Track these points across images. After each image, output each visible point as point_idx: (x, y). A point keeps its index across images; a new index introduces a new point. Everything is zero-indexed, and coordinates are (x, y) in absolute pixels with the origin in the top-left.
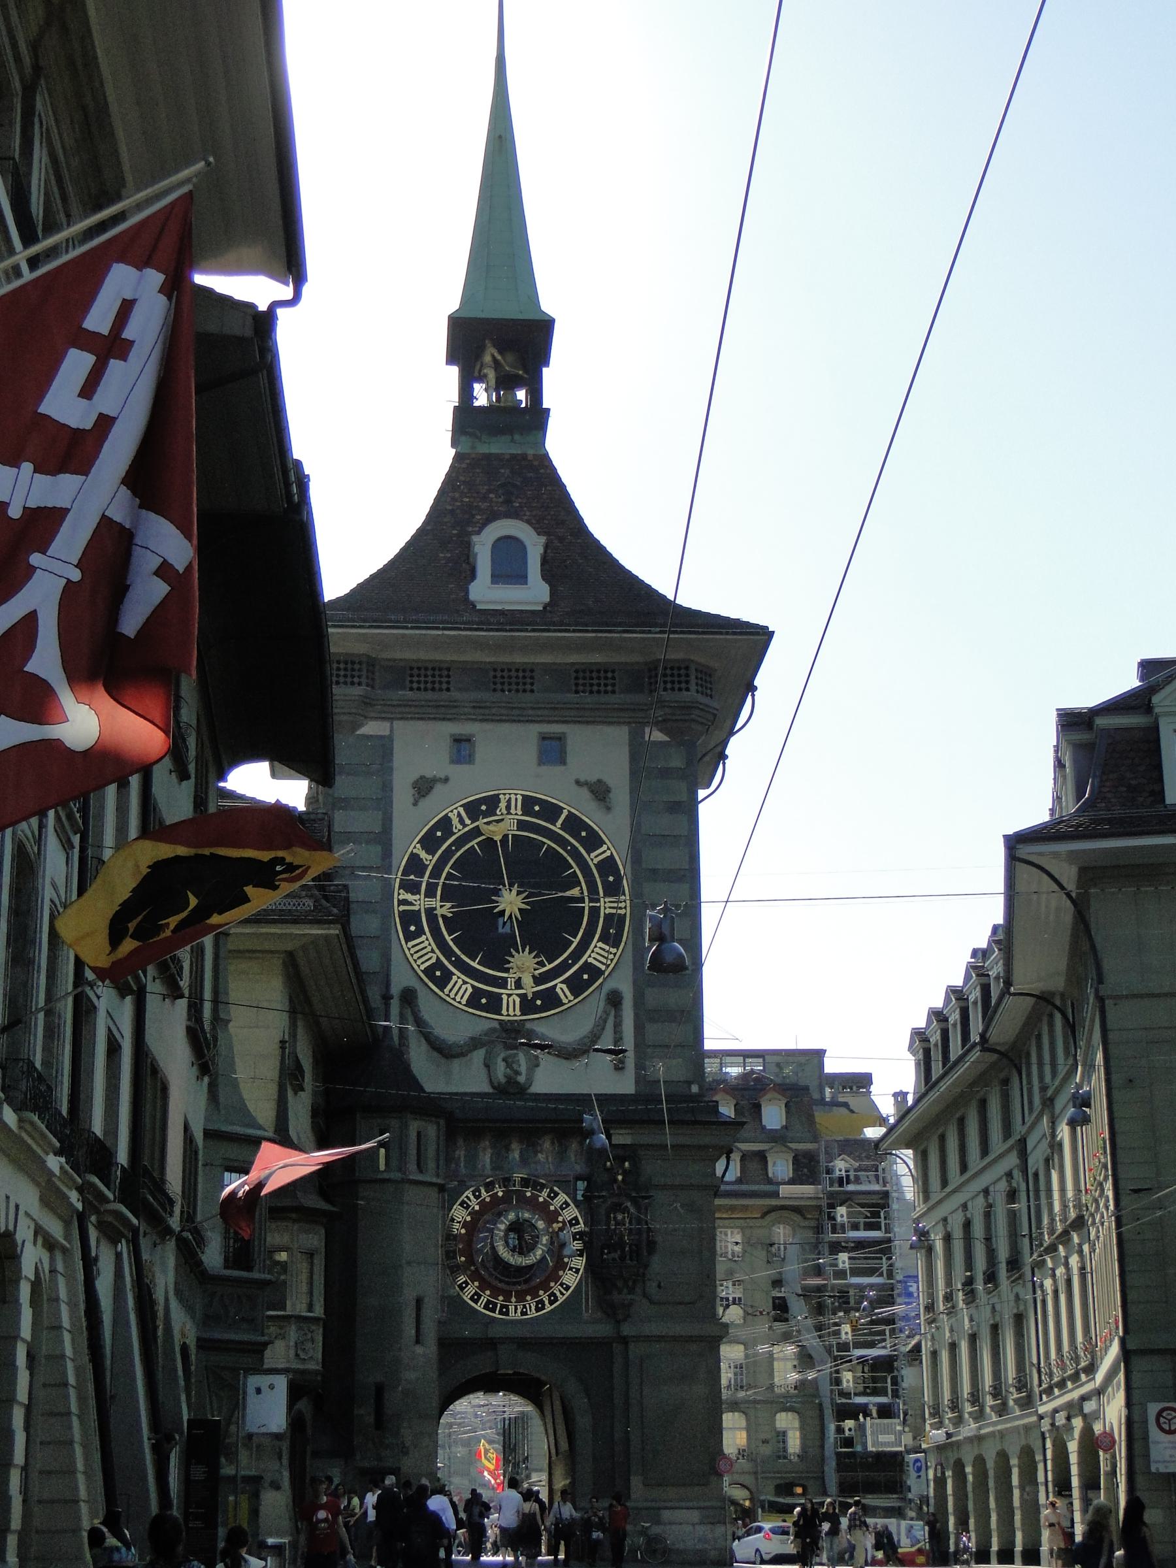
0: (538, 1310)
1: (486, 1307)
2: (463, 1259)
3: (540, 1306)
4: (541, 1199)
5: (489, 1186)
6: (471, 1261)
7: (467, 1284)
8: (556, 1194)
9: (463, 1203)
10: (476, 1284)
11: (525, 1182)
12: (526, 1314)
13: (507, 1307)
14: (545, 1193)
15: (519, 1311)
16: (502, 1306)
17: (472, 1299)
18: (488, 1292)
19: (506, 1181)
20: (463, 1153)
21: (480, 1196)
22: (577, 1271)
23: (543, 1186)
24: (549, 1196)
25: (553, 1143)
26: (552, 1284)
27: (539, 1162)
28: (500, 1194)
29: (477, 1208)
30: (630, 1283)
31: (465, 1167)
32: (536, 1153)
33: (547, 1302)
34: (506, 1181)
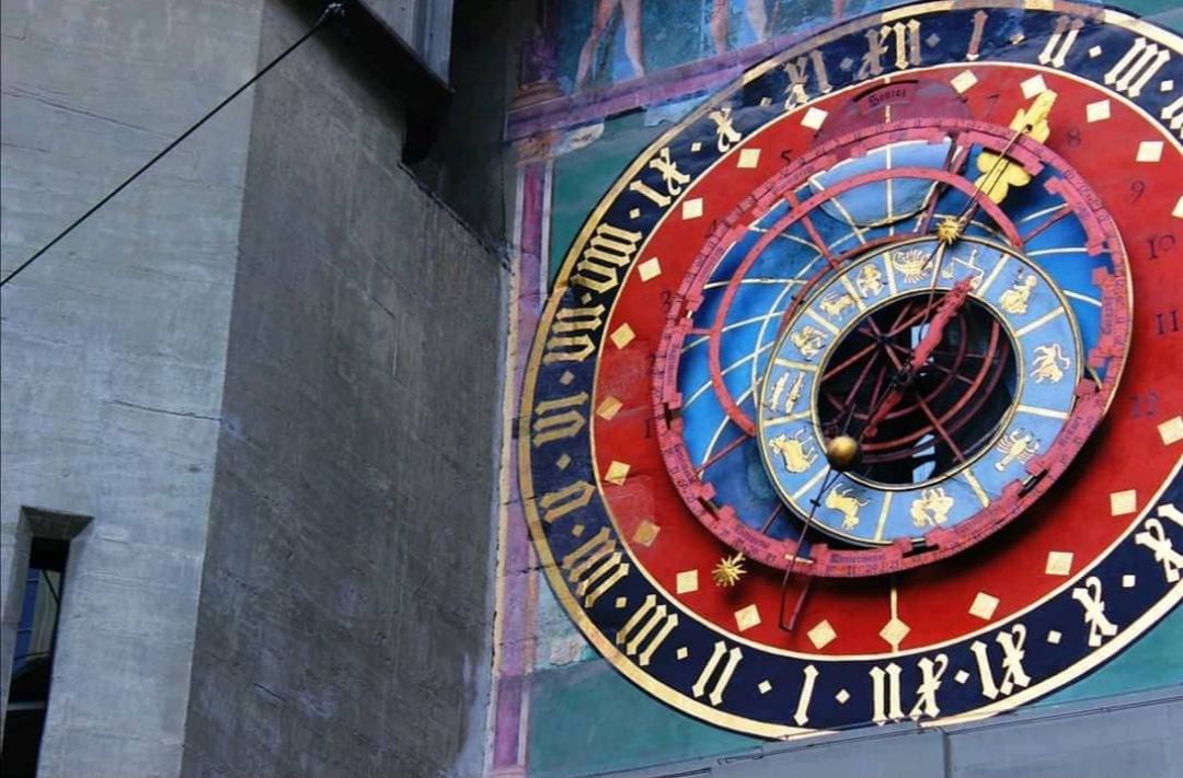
0: (1040, 663)
1: (739, 699)
2: (619, 470)
3: (1055, 639)
6: (652, 472)
7: (634, 588)
8: (1118, 44)
12: (972, 697)
13: (858, 678)
14: (1055, 52)
15: (930, 686)
16: (831, 677)
17: (662, 667)
21: (710, 152)
24: (1077, 63)
26: (1123, 502)
28: (815, 119)
29: (694, 209)
31: (643, 44)
33: (1095, 611)
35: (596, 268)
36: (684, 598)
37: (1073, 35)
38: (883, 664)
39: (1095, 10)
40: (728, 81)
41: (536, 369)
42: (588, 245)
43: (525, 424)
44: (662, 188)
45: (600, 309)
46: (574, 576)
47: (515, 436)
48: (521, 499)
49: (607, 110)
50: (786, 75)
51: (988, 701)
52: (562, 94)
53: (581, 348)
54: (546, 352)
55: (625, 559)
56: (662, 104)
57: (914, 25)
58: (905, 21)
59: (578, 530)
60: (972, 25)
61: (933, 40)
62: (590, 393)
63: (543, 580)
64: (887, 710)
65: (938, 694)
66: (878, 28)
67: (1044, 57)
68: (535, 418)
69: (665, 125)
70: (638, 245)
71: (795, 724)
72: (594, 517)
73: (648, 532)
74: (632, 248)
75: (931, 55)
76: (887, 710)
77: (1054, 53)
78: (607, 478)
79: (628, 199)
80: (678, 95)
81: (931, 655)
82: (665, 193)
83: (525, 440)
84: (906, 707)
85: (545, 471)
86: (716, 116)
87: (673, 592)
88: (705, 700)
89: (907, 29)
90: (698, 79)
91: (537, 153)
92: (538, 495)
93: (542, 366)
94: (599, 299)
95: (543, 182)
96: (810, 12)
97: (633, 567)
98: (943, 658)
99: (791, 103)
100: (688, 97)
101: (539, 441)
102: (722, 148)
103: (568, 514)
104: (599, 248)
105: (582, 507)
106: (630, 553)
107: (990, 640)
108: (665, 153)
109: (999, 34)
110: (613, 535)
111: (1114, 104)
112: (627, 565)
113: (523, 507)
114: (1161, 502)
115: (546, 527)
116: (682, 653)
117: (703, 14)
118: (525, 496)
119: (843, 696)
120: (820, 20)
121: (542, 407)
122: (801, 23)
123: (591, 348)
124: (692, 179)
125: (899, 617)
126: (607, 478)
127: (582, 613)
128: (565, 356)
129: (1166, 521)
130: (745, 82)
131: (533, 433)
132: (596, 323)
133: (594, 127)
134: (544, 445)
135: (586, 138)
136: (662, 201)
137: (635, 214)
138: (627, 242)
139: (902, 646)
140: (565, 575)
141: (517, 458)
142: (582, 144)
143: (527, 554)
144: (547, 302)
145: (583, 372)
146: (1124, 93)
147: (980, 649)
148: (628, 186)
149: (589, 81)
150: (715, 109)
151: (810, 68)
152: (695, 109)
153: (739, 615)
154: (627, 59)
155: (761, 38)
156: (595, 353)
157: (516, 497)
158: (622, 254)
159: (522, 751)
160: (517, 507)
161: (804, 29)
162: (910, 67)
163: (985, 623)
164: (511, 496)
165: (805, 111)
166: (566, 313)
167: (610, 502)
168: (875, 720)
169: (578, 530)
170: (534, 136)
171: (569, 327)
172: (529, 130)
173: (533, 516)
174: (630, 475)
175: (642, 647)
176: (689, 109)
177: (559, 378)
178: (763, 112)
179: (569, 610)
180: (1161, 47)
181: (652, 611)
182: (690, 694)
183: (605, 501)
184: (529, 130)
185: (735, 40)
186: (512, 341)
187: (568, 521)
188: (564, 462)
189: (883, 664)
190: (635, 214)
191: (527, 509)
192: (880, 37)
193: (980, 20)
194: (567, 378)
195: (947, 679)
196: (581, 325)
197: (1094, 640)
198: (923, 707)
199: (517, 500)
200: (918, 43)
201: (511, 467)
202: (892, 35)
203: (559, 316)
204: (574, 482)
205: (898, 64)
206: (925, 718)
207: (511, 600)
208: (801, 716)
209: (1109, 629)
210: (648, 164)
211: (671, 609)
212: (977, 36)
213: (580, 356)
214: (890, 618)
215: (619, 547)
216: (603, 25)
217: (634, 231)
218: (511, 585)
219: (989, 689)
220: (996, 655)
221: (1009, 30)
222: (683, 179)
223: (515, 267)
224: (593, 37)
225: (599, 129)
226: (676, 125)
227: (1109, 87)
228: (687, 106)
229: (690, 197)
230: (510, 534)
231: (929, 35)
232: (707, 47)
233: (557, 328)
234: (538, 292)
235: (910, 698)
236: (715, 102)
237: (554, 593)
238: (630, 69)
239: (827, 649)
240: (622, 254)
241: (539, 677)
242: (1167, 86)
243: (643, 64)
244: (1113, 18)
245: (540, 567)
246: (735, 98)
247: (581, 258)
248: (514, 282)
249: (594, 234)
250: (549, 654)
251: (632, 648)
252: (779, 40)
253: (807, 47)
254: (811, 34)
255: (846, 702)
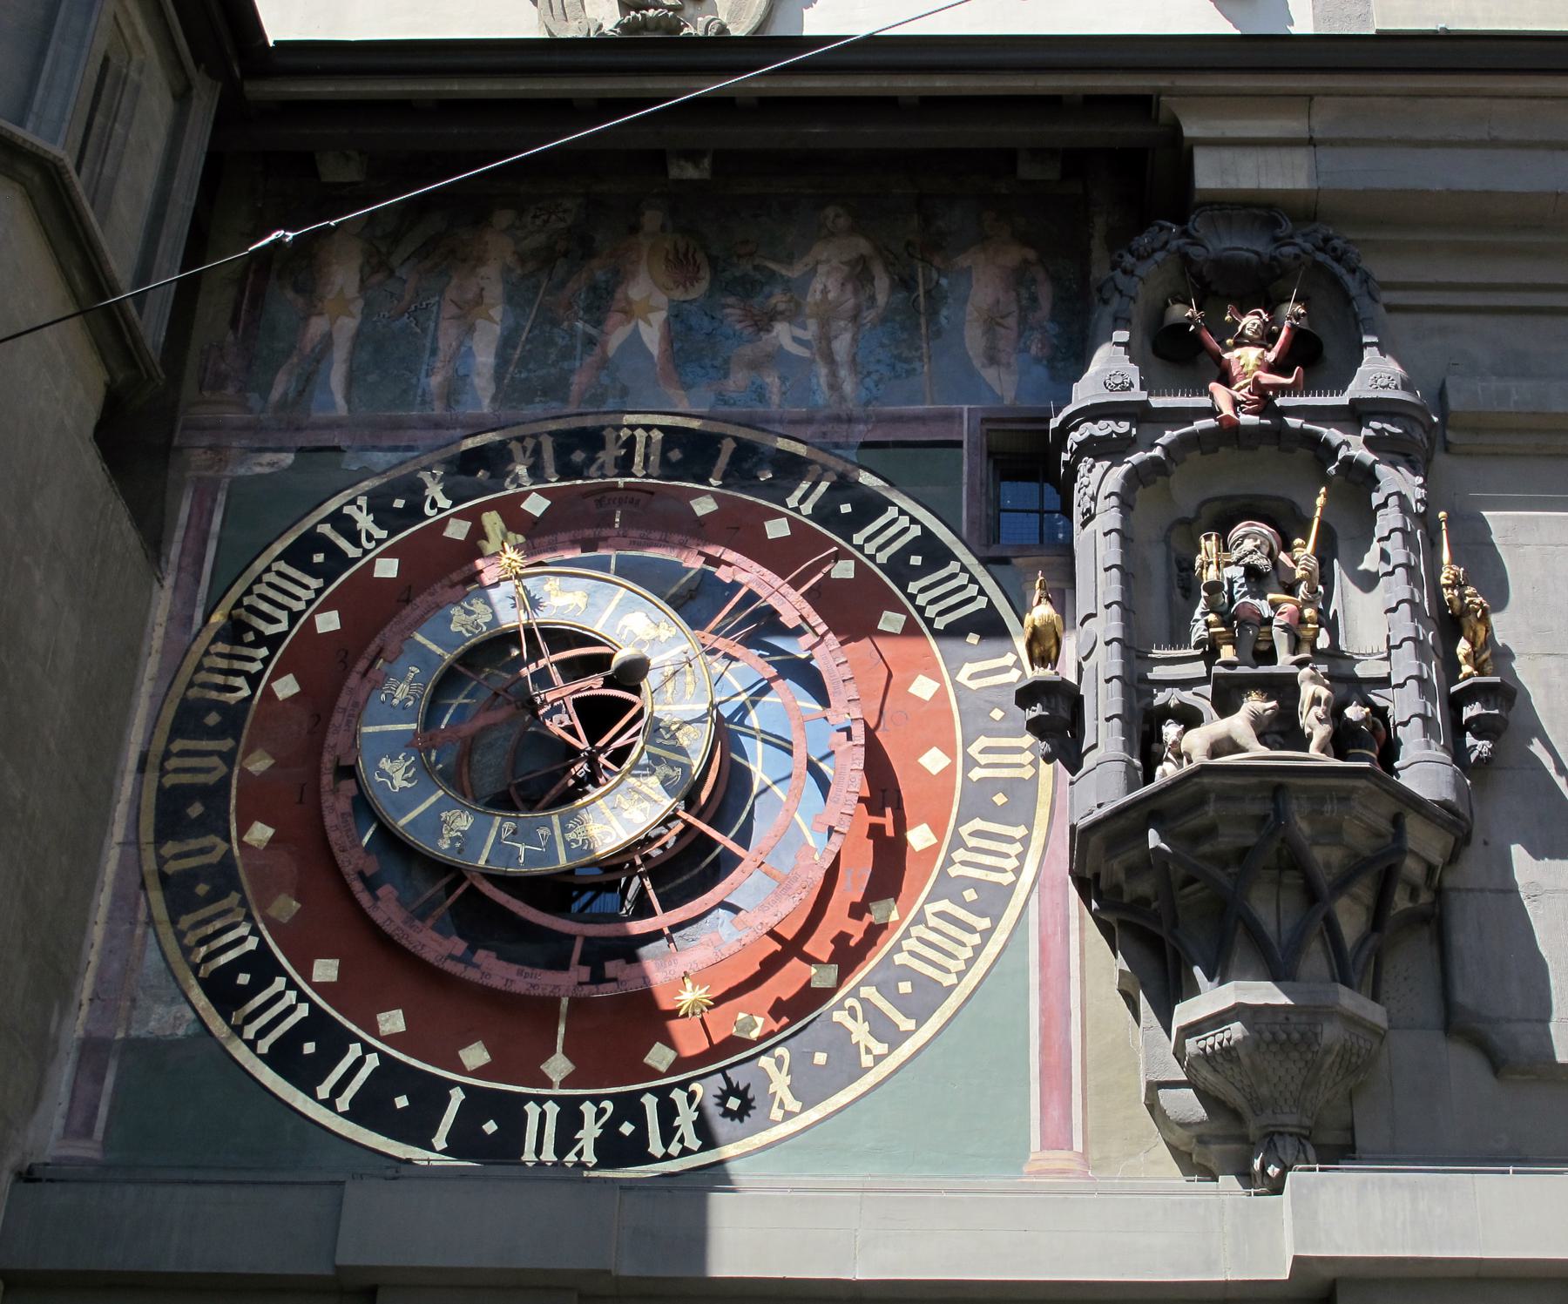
2: (260, 833)
4: (777, 529)
5: (475, 469)
7: (262, 966)
8: (870, 507)
9: (312, 541)
10: (326, 970)
11: (691, 452)
12: (636, 1151)
13: (511, 1112)
14: (803, 500)
15: (590, 1133)
17: (283, 1058)
18: (393, 1021)
19: (578, 446)
20: (348, 325)
21: (414, 512)
22: (993, 899)
23: (791, 469)
24: (825, 513)
25: (860, 275)
27: (778, 357)
29: (388, 569)
30: (1351, 919)
31: (351, 380)
32: (764, 321)
34: (578, 446)
35: (265, 607)
36: (320, 988)
37: (823, 486)
38: (540, 1100)
39: (849, 467)
40: (441, 442)
41: (177, 701)
42: (258, 580)
43: (154, 760)
44: (354, 539)
45: (263, 652)
46: (190, 939)
47: (142, 767)
48: (137, 843)
49: (302, 440)
50: (510, 452)
51: (652, 1159)
52: (250, 411)
53: (237, 689)
54: (191, 685)
55: (255, 931)
56: (364, 449)
57: (657, 435)
58: (648, 428)
59: (202, 889)
60: (719, 451)
61: (676, 455)
62: (238, 741)
63: (152, 939)
64: (539, 1150)
65: (598, 1142)
66: (619, 428)
67: (792, 501)
68: (167, 755)
69: (366, 473)
70: (319, 592)
71: (432, 1149)
72: (224, 878)
73: (287, 907)
74: (311, 595)
75: (670, 470)
76: (539, 1150)
77: (803, 500)
78: (246, 838)
79: (312, 541)
80: (386, 443)
81: (596, 1100)
82: (356, 542)
83: (152, 777)
84: (562, 1148)
85: (174, 813)
86: (425, 476)
87: (307, 977)
88: (329, 1104)
89: (649, 438)
90: (410, 432)
91: (210, 467)
92: (161, 837)
93: (184, 700)
94: (261, 640)
95: (214, 500)
96: (545, 394)
97: (262, 942)
98: (608, 1105)
99: (512, 482)
100: (395, 449)
101: (170, 780)
102: (427, 510)
103: (192, 869)
104: (271, 585)
105: (210, 865)
106: (262, 926)
107: (663, 1093)
108: (362, 501)
109: (746, 466)
110: (243, 902)
111: (859, 565)
112: (257, 939)
113: (139, 849)
114: (862, 983)
115: (164, 879)
116: (309, 1048)
117: (425, 367)
118: (143, 839)
119: (490, 1127)
120: (554, 404)
121: (178, 745)
122: (532, 402)
123: (246, 692)
124: (390, 536)
125: (565, 1052)
126: (246, 838)
127: (193, 981)
128: (214, 695)
129: (865, 1002)
130: (463, 448)
131: (163, 772)
132: (257, 666)
133: (282, 456)
134: (175, 787)
135: (271, 464)
136: (353, 552)
137: (319, 558)
138: (306, 587)
139: (563, 1085)
140: (180, 935)
141: (140, 796)
142: (267, 470)
143: (137, 904)
144: (200, 631)
145: (233, 718)
146: (872, 558)
147: (650, 1102)
148: (315, 526)
149: (283, 404)
150: (428, 468)
151: (537, 451)
152: (402, 463)
153: (381, 1017)
154: (331, 393)
155: (486, 407)
156: (250, 699)
157: (132, 837)
158: (298, 599)
159: (100, 1124)
160: (132, 850)
161: (537, 409)
162: (647, 476)
163: (658, 1075)
164: (126, 836)
165: (527, 494)
166: (221, 647)
167: (246, 866)
168: (524, 1158)
169: (202, 889)
170: (210, 448)
171: (223, 664)
172: (206, 441)
173: (150, 864)
174: (272, 840)
175: (262, 1033)
176: (395, 461)
177: (203, 717)
178: (480, 483)
179: (180, 977)
180: (914, 521)
181: (279, 996)
182: (313, 1096)
183: (239, 863)
184: (206, 441)
185: (458, 402)
186: (151, 666)
187: (192, 876)
188: (196, 810)
189: (540, 1100)
190: (319, 558)
191: (144, 854)
192: (619, 437)
193: (728, 447)
194: (213, 719)
195: (611, 1128)
196: (237, 665)
197: (776, 1114)
198: (580, 1154)
199: (133, 841)
200: (658, 453)
201: (131, 802)
202: (632, 439)
203: (213, 649)
204: (204, 835)
205: (634, 470)
206: (581, 1165)
207: (108, 952)
208: (440, 1142)
209: (793, 1105)
210: (341, 508)
211: (302, 997)
212: (723, 461)
213: (232, 698)
214: (554, 1052)
215: (249, 917)
216: (308, 350)
217: (315, 576)
218: (110, 934)
219: (656, 1148)
220: (668, 1112)
221: (760, 464)
222: (384, 534)
223: (169, 581)
224: (295, 360)
225: (288, 459)
226: (378, 474)
227: (855, 547)
228: (393, 457)
229: (383, 555)
230: (119, 876)
231: (672, 449)
232: (424, 402)
233: (207, 662)
234: (191, 618)
235: (565, 1142)
236: (425, 460)
237: (164, 955)
238: (333, 405)
239: (477, 1073)
240: (298, 599)
241: (133, 1045)
242: (916, 560)
243: (348, 401)
244: (866, 478)
245: (151, 921)
246: (447, 462)
247: (249, 592)
248: (163, 602)
249: (268, 569)
250: (147, 1024)
251: (250, 1032)
252: (506, 414)
253: (536, 428)
254: (545, 419)
255: (491, 1136)
